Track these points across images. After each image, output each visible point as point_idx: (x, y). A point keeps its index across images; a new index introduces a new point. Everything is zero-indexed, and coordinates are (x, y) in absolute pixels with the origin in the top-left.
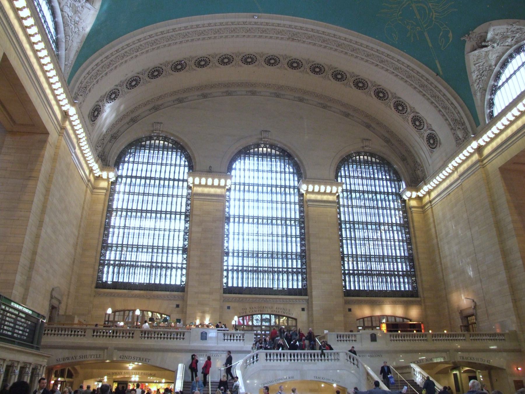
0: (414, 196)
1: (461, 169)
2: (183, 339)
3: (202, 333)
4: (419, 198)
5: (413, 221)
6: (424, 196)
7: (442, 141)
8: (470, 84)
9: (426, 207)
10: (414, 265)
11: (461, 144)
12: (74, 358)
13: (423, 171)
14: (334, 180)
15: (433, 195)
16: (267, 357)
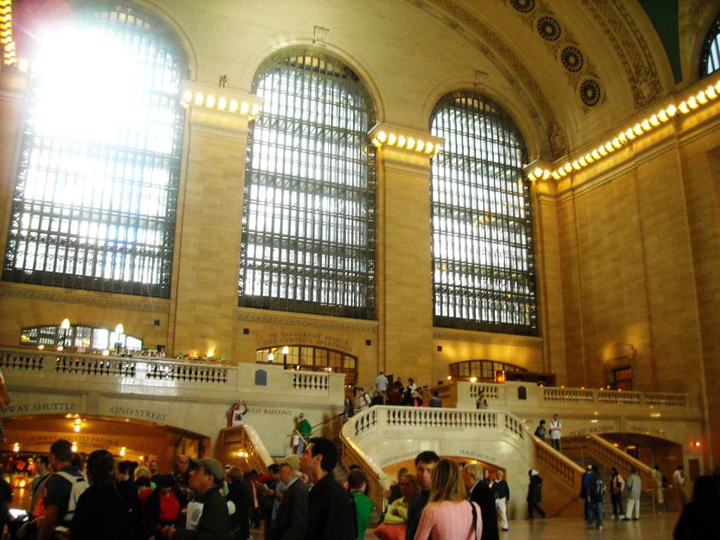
0: (546, 177)
1: (639, 145)
2: (224, 381)
3: (257, 373)
4: (552, 180)
5: (540, 217)
6: (563, 178)
7: (610, 95)
8: (679, 15)
9: (564, 197)
10: (535, 284)
11: (644, 105)
12: (24, 409)
13: (564, 140)
14: (424, 131)
15: (579, 179)
16: (389, 416)
